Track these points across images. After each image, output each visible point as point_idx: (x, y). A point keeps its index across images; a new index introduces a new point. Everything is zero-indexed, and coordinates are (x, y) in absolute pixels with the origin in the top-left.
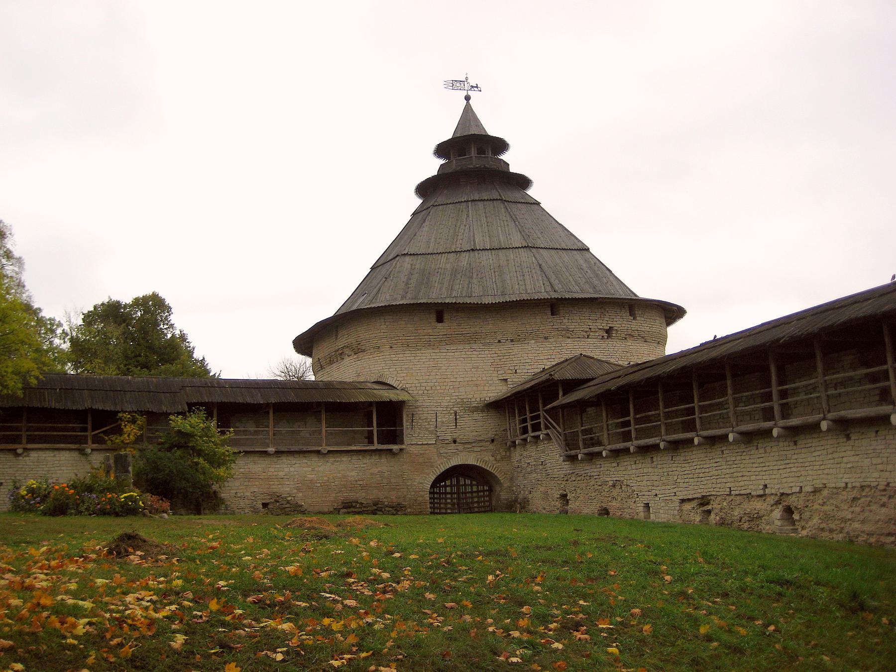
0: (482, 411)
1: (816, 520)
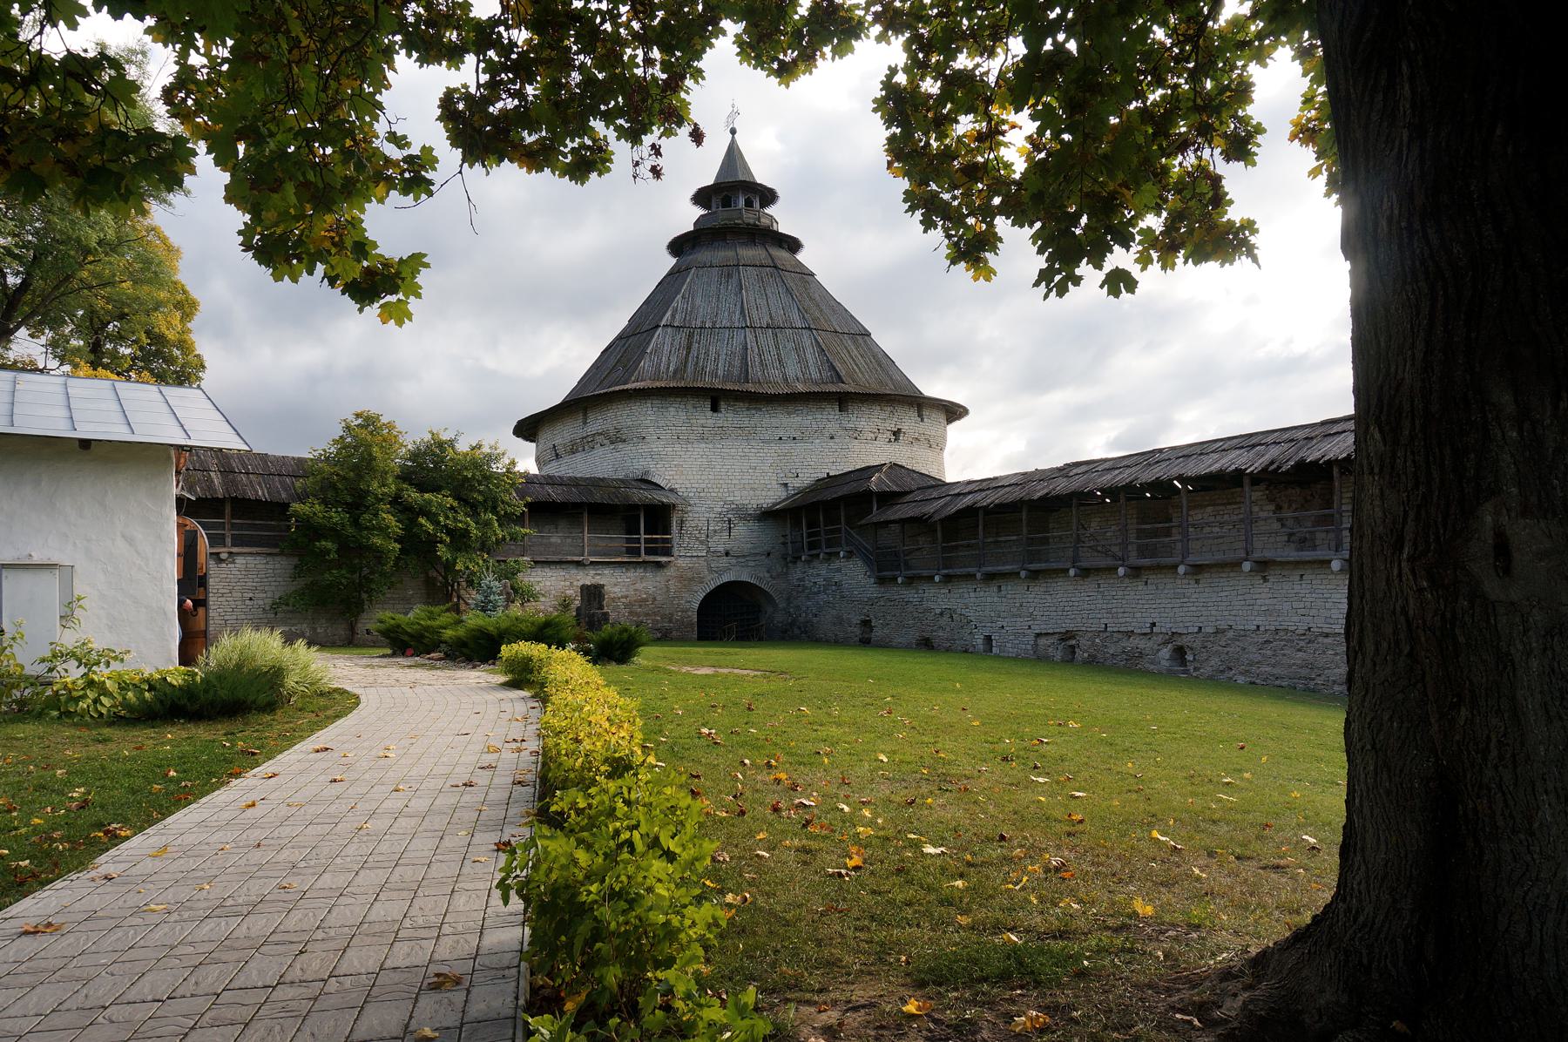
1: (1214, 661)
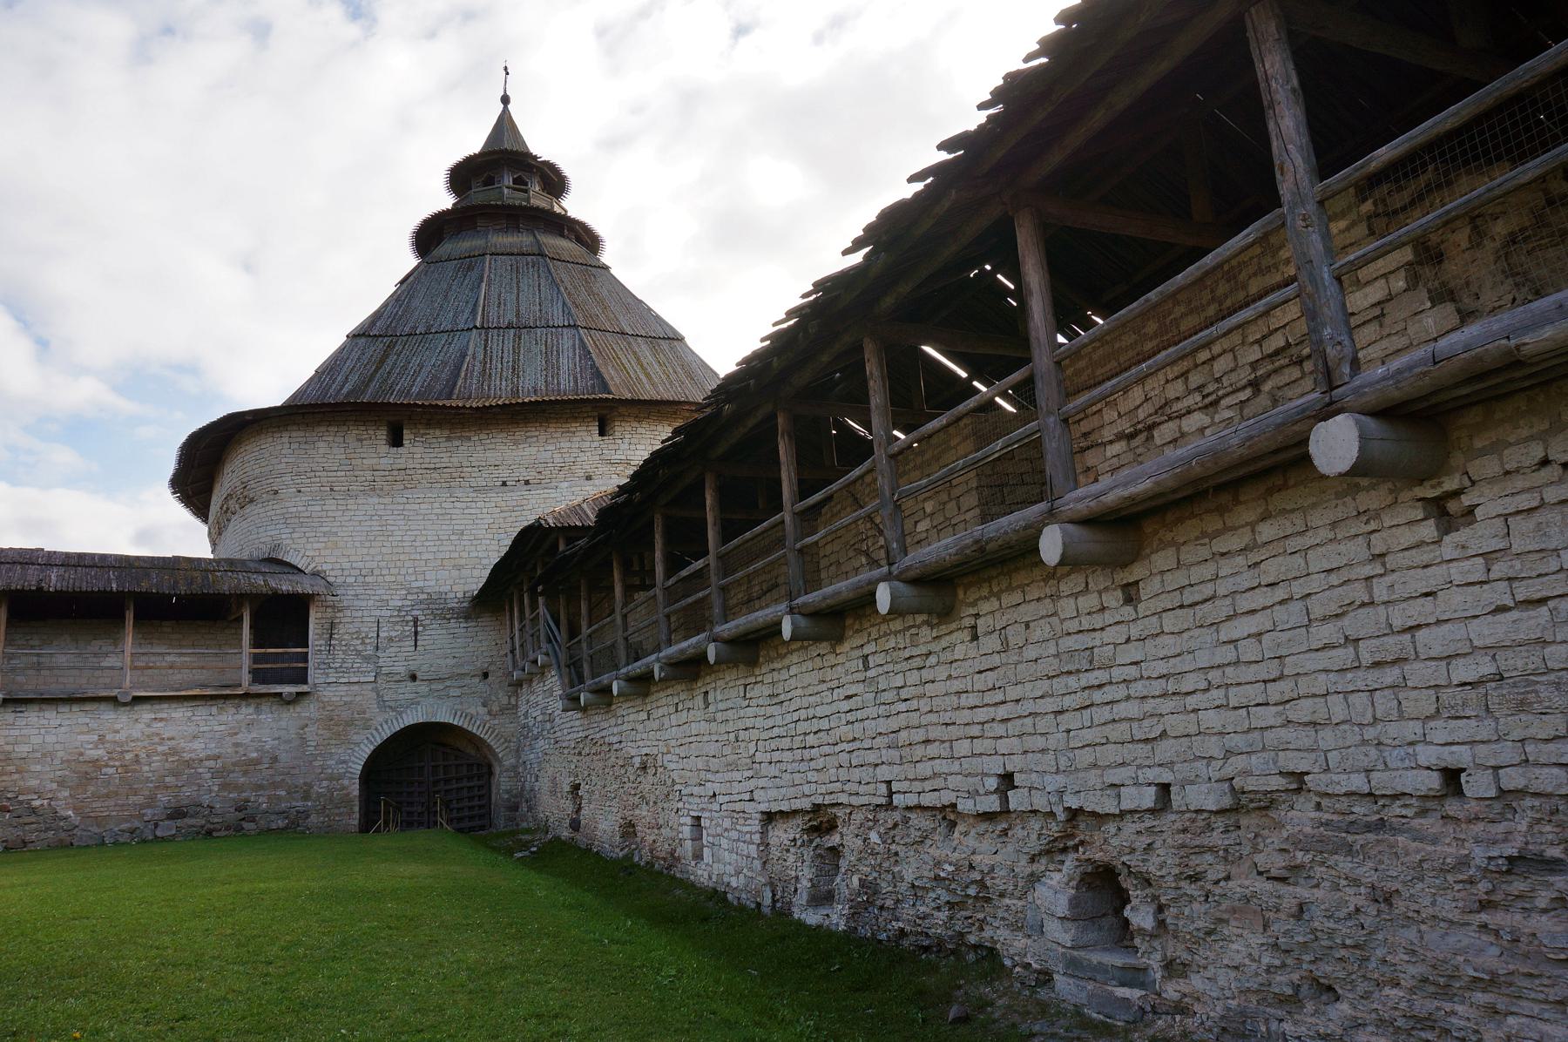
0: (467, 618)
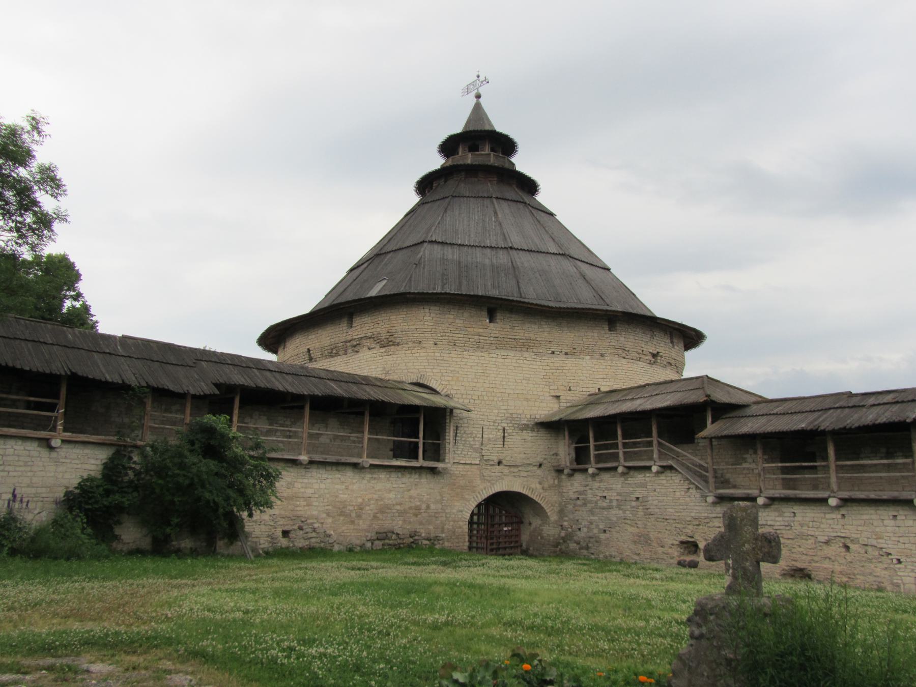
0: (532, 430)
